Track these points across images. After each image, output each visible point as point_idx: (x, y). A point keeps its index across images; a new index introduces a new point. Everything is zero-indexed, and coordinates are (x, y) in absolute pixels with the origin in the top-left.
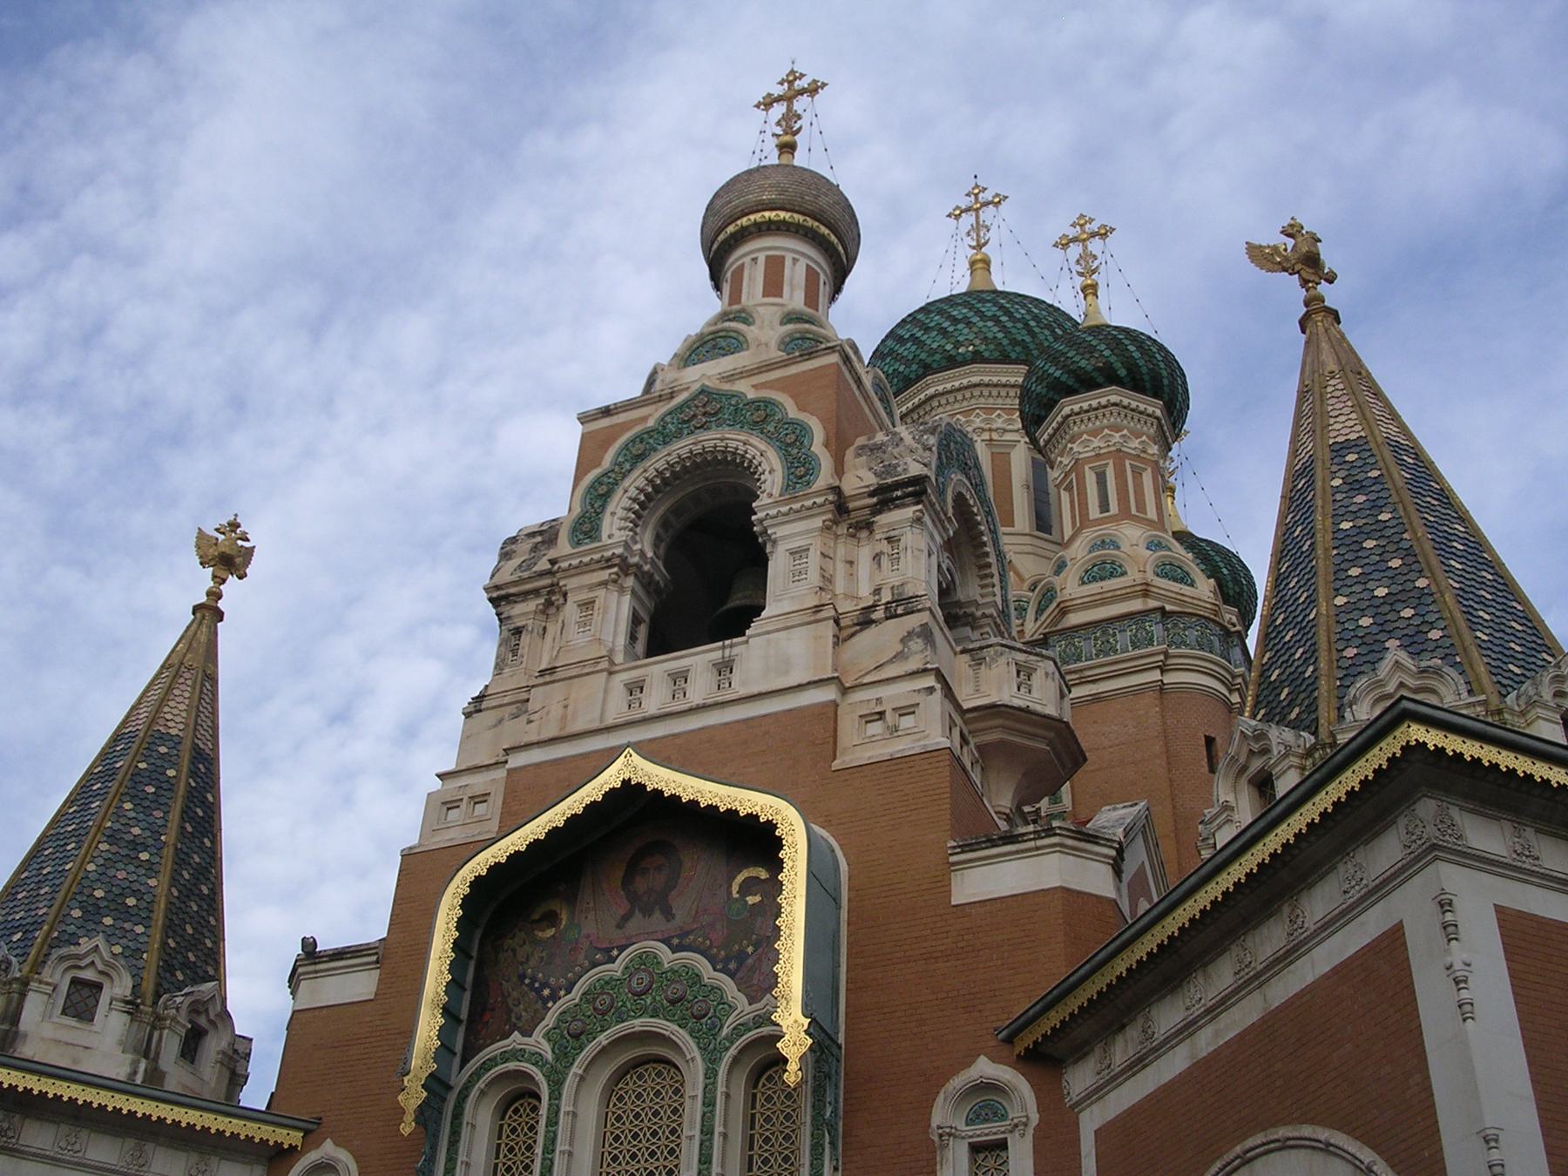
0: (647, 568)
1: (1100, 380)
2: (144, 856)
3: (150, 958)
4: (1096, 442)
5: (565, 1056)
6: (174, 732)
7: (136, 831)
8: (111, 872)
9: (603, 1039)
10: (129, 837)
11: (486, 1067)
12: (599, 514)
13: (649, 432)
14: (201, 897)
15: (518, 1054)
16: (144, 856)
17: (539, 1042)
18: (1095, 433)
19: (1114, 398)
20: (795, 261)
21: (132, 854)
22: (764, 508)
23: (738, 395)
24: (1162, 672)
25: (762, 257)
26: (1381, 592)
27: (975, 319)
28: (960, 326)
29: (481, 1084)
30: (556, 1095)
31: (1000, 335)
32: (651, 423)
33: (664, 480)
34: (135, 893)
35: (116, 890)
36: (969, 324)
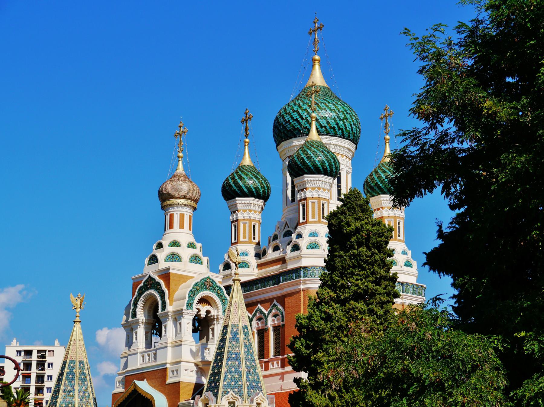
1: (301, 173)
6: (73, 359)
7: (69, 388)
8: (65, 400)
10: (68, 390)
12: (136, 309)
13: (141, 287)
14: (86, 397)
16: (71, 394)
20: (177, 213)
21: (69, 394)
23: (154, 280)
25: (169, 214)
26: (216, 371)
27: (291, 121)
28: (287, 124)
31: (299, 126)
32: (142, 284)
33: (147, 299)
34: (71, 403)
35: (67, 404)
36: (290, 123)
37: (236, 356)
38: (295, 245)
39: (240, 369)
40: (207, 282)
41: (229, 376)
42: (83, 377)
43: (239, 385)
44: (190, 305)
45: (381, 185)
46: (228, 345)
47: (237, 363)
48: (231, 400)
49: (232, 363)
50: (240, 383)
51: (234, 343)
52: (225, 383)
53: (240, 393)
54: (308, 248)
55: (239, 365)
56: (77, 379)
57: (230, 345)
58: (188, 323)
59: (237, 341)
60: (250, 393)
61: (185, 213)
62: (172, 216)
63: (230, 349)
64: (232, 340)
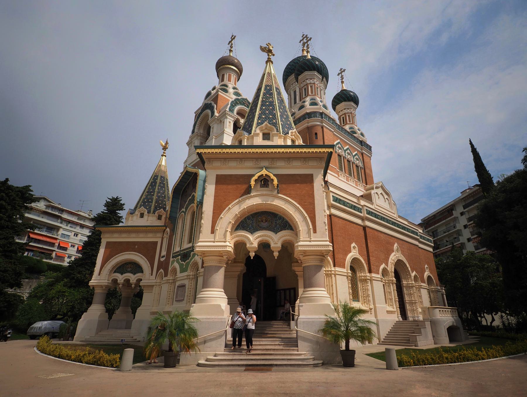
0: (202, 135)
2: (152, 193)
3: (153, 207)
4: (304, 83)
5: (186, 210)
9: (189, 208)
11: (180, 213)
13: (200, 113)
15: (183, 212)
16: (152, 193)
17: (184, 210)
18: (304, 82)
19: (306, 74)
22: (209, 122)
24: (308, 123)
29: (179, 217)
30: (185, 217)
37: (270, 103)
38: (302, 106)
39: (274, 112)
40: (245, 102)
41: (263, 117)
42: (162, 185)
43: (273, 123)
44: (231, 110)
45: (344, 96)
46: (262, 97)
47: (271, 108)
48: (266, 131)
49: (266, 108)
50: (274, 121)
51: (268, 95)
52: (259, 121)
53: (275, 125)
54: (310, 105)
55: (274, 109)
56: (157, 185)
57: (264, 97)
58: (230, 122)
59: (271, 94)
60: (284, 130)
61: (232, 75)
62: (223, 76)
63: (264, 99)
64: (266, 94)
